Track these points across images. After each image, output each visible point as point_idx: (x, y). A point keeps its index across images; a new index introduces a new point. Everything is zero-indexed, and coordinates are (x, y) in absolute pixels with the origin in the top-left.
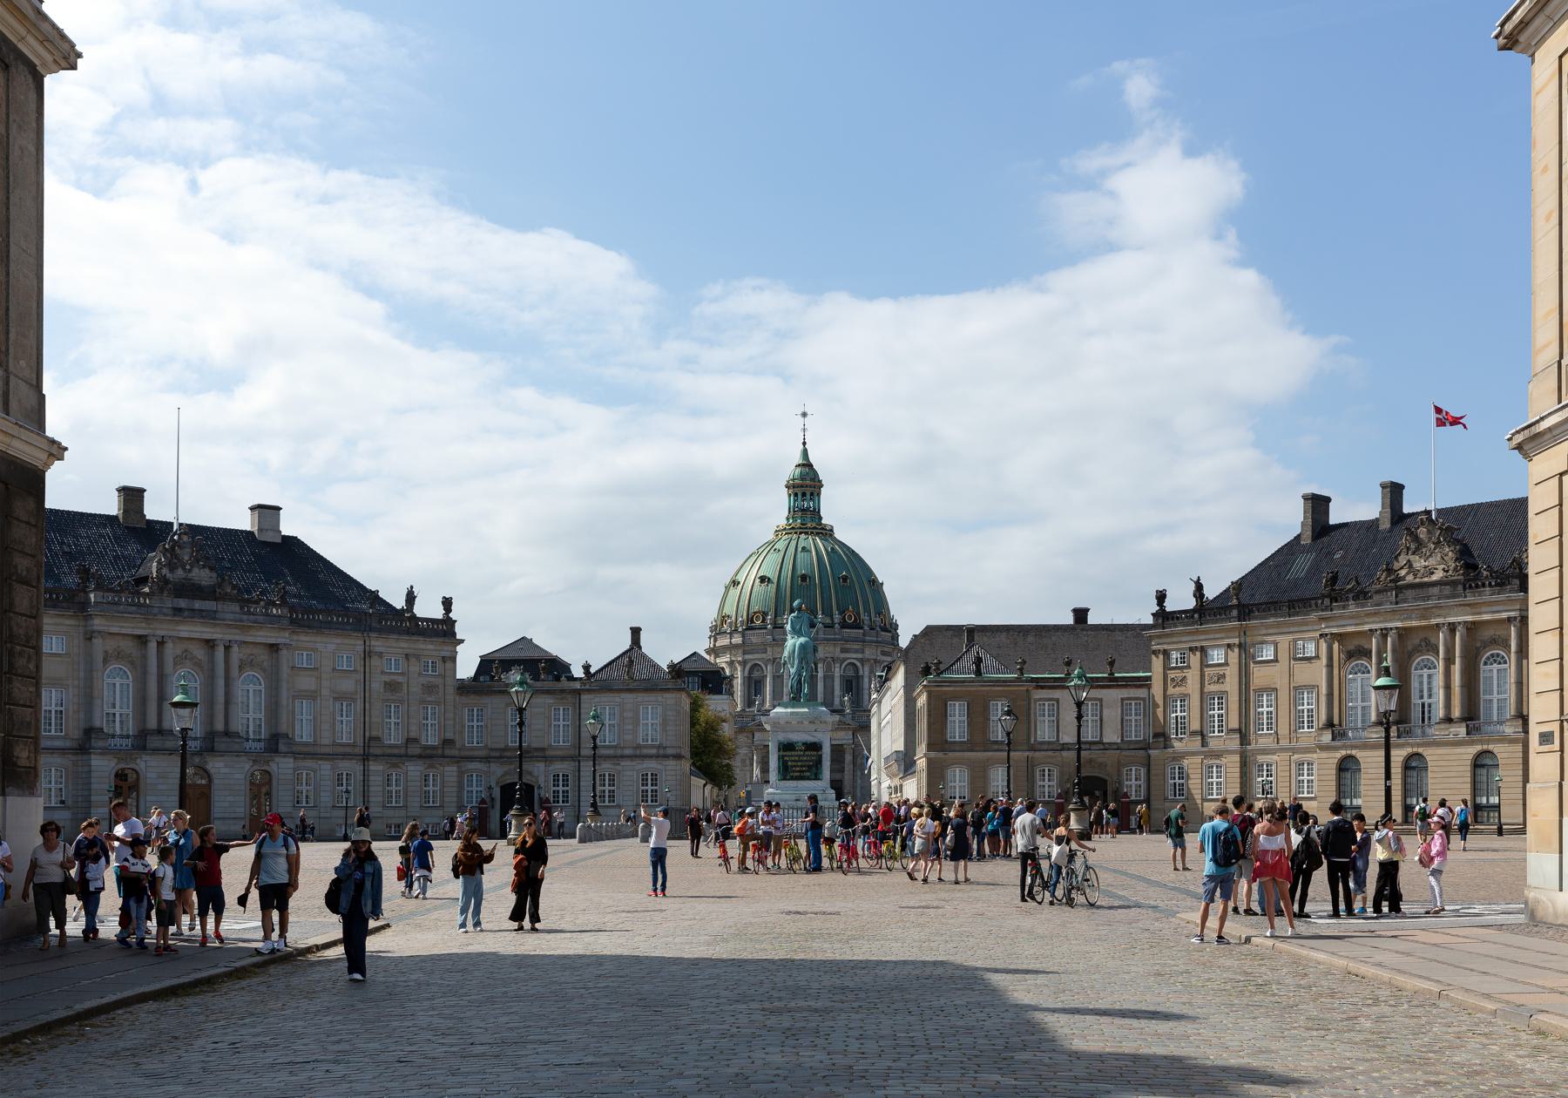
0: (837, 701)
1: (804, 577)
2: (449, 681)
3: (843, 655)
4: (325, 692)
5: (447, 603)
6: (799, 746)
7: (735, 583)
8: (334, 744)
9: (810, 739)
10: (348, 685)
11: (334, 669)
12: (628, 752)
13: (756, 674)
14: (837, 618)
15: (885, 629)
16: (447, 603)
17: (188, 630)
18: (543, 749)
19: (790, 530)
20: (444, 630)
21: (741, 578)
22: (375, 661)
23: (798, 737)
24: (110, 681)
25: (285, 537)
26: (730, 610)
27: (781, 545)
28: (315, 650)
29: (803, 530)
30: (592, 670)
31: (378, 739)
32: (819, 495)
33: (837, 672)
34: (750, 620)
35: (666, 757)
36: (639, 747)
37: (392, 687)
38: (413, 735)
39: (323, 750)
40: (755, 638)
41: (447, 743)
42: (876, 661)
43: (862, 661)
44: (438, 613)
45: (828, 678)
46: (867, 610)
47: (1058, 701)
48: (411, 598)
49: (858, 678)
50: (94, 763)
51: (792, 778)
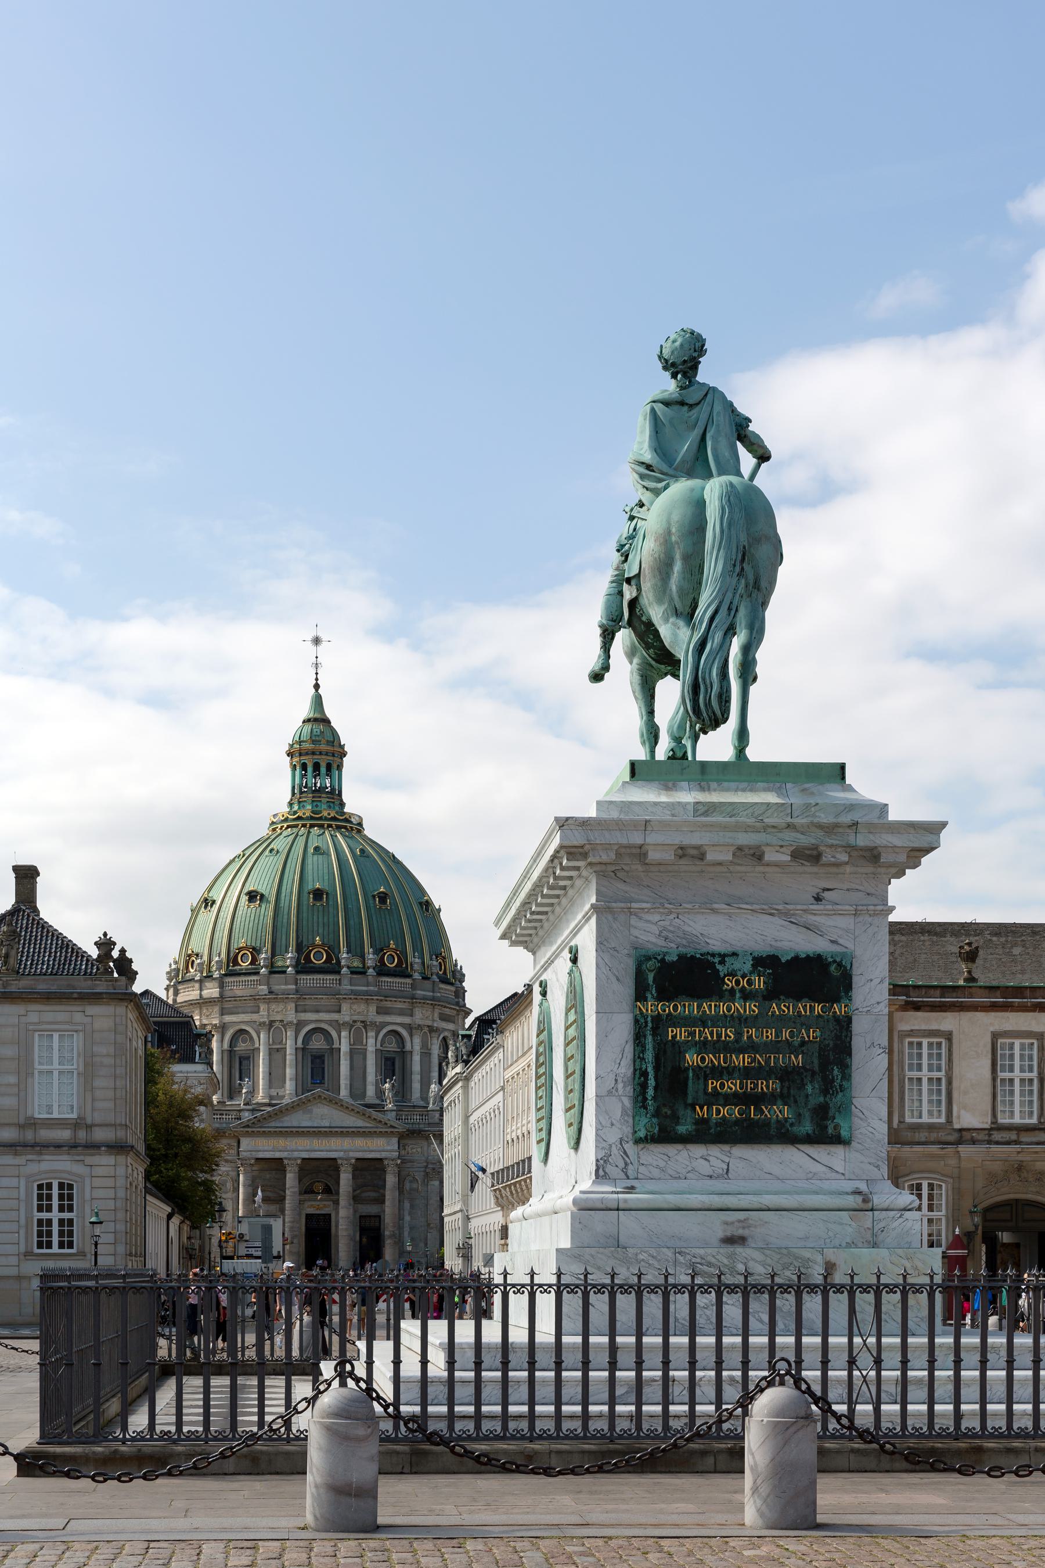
0: (371, 1091)
1: (318, 894)
3: (380, 1019)
6: (741, 974)
7: (207, 903)
9: (793, 941)
13: (241, 1047)
14: (371, 958)
15: (445, 980)
19: (293, 822)
21: (217, 895)
23: (736, 930)
26: (200, 944)
27: (281, 844)
29: (316, 821)
32: (340, 767)
33: (371, 1045)
34: (233, 960)
40: (238, 988)
42: (432, 1029)
43: (410, 1028)
45: (357, 1054)
46: (417, 947)
47: (949, 1036)
49: (404, 1054)
51: (707, 1134)
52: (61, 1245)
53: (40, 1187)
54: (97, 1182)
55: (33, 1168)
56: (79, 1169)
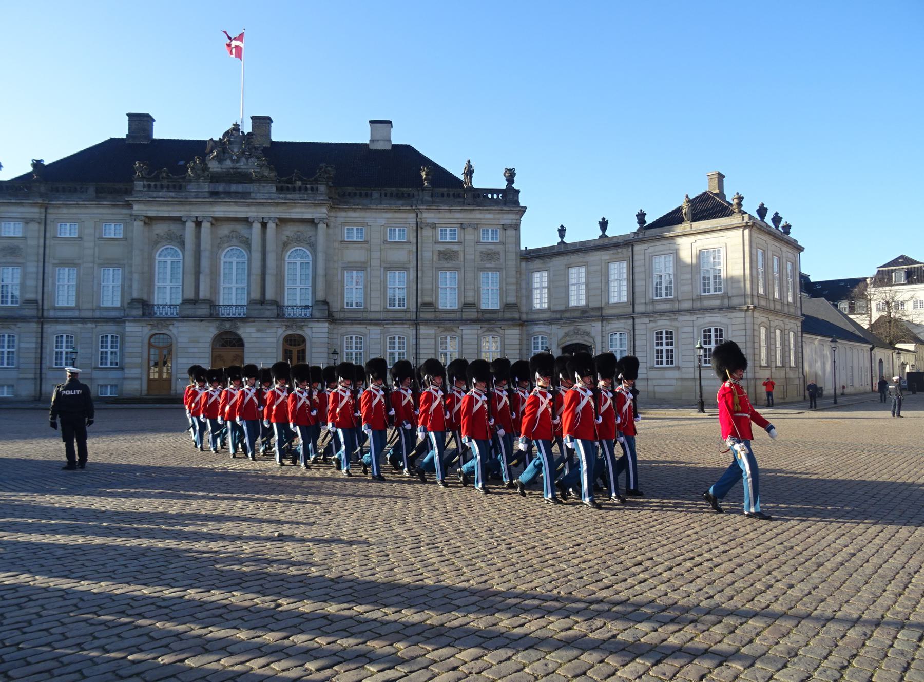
2: (511, 247)
4: (375, 262)
5: (510, 176)
8: (388, 311)
10: (401, 255)
11: (385, 242)
12: (686, 305)
16: (510, 176)
17: (221, 210)
18: (601, 309)
20: (509, 199)
22: (427, 232)
24: (162, 259)
25: (393, 146)
28: (364, 224)
30: (649, 220)
31: (430, 304)
35: (732, 308)
36: (700, 298)
37: (447, 256)
38: (470, 300)
39: (372, 316)
41: (508, 306)
44: (503, 185)
48: (469, 172)
50: (128, 329)
52: (667, 363)
53: (705, 331)
54: (735, 327)
55: (701, 321)
56: (725, 320)
